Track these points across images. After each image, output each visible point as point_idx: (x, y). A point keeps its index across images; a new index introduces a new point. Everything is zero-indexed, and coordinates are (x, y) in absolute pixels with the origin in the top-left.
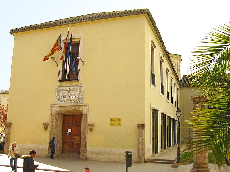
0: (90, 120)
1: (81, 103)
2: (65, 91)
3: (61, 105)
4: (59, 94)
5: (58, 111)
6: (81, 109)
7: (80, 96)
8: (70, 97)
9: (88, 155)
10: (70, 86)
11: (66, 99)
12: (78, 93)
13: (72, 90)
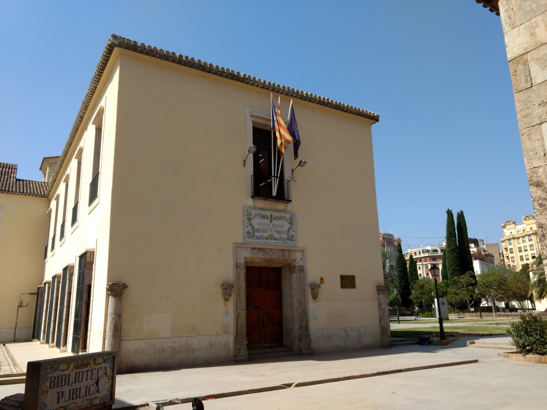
0: (312, 276)
1: (293, 245)
2: (264, 218)
3: (257, 246)
4: (252, 222)
5: (247, 257)
6: (293, 257)
7: (291, 231)
8: (274, 232)
10: (272, 210)
11: (266, 235)
13: (278, 218)
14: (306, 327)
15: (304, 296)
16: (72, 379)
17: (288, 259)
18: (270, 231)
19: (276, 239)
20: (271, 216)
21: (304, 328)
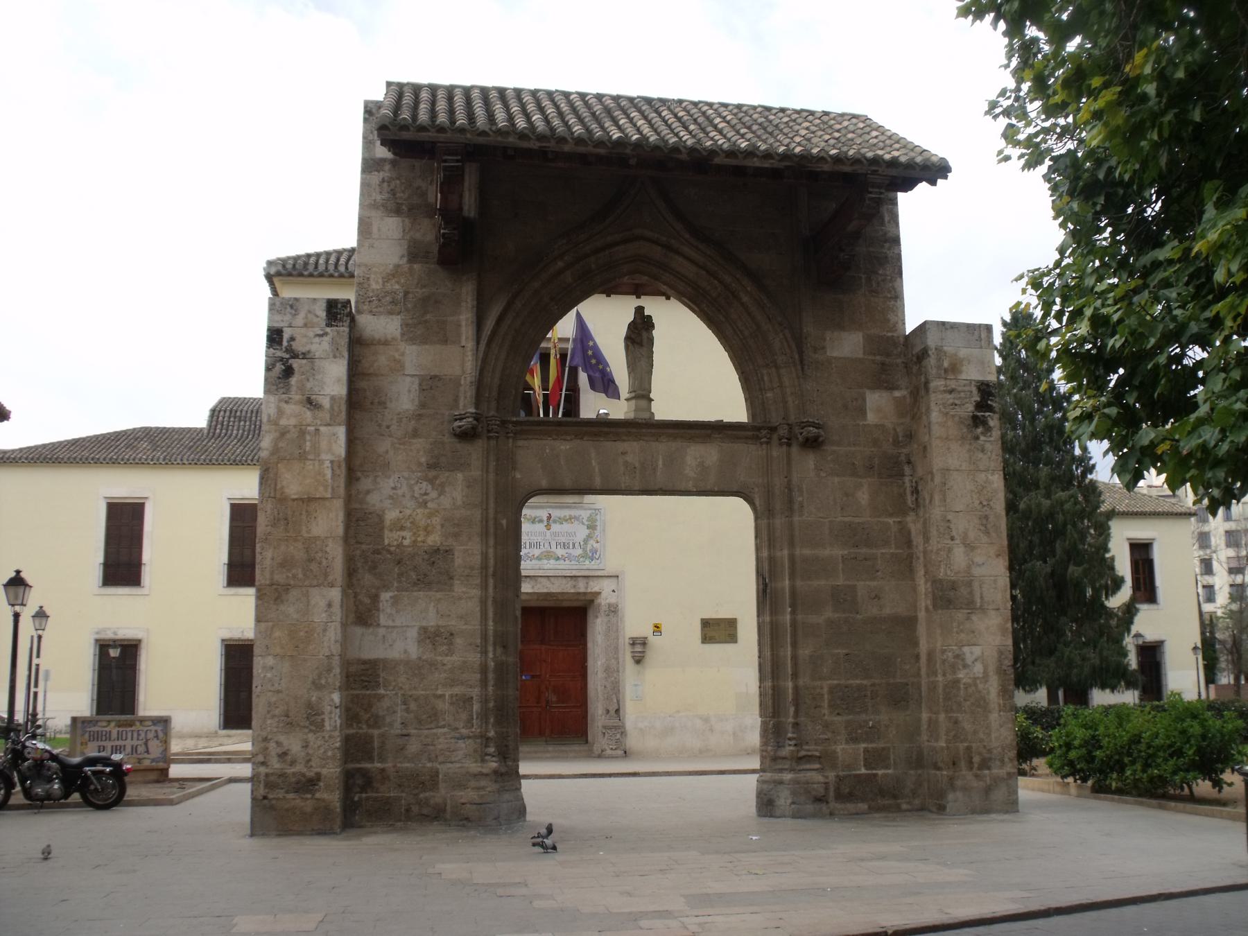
0: (635, 624)
6: (596, 589)
7: (592, 542)
8: (553, 546)
9: (632, 742)
12: (582, 532)
13: (561, 521)
14: (617, 711)
15: (617, 659)
16: (114, 735)
17: (585, 594)
18: (547, 545)
19: (558, 559)
20: (549, 517)
21: (612, 712)
